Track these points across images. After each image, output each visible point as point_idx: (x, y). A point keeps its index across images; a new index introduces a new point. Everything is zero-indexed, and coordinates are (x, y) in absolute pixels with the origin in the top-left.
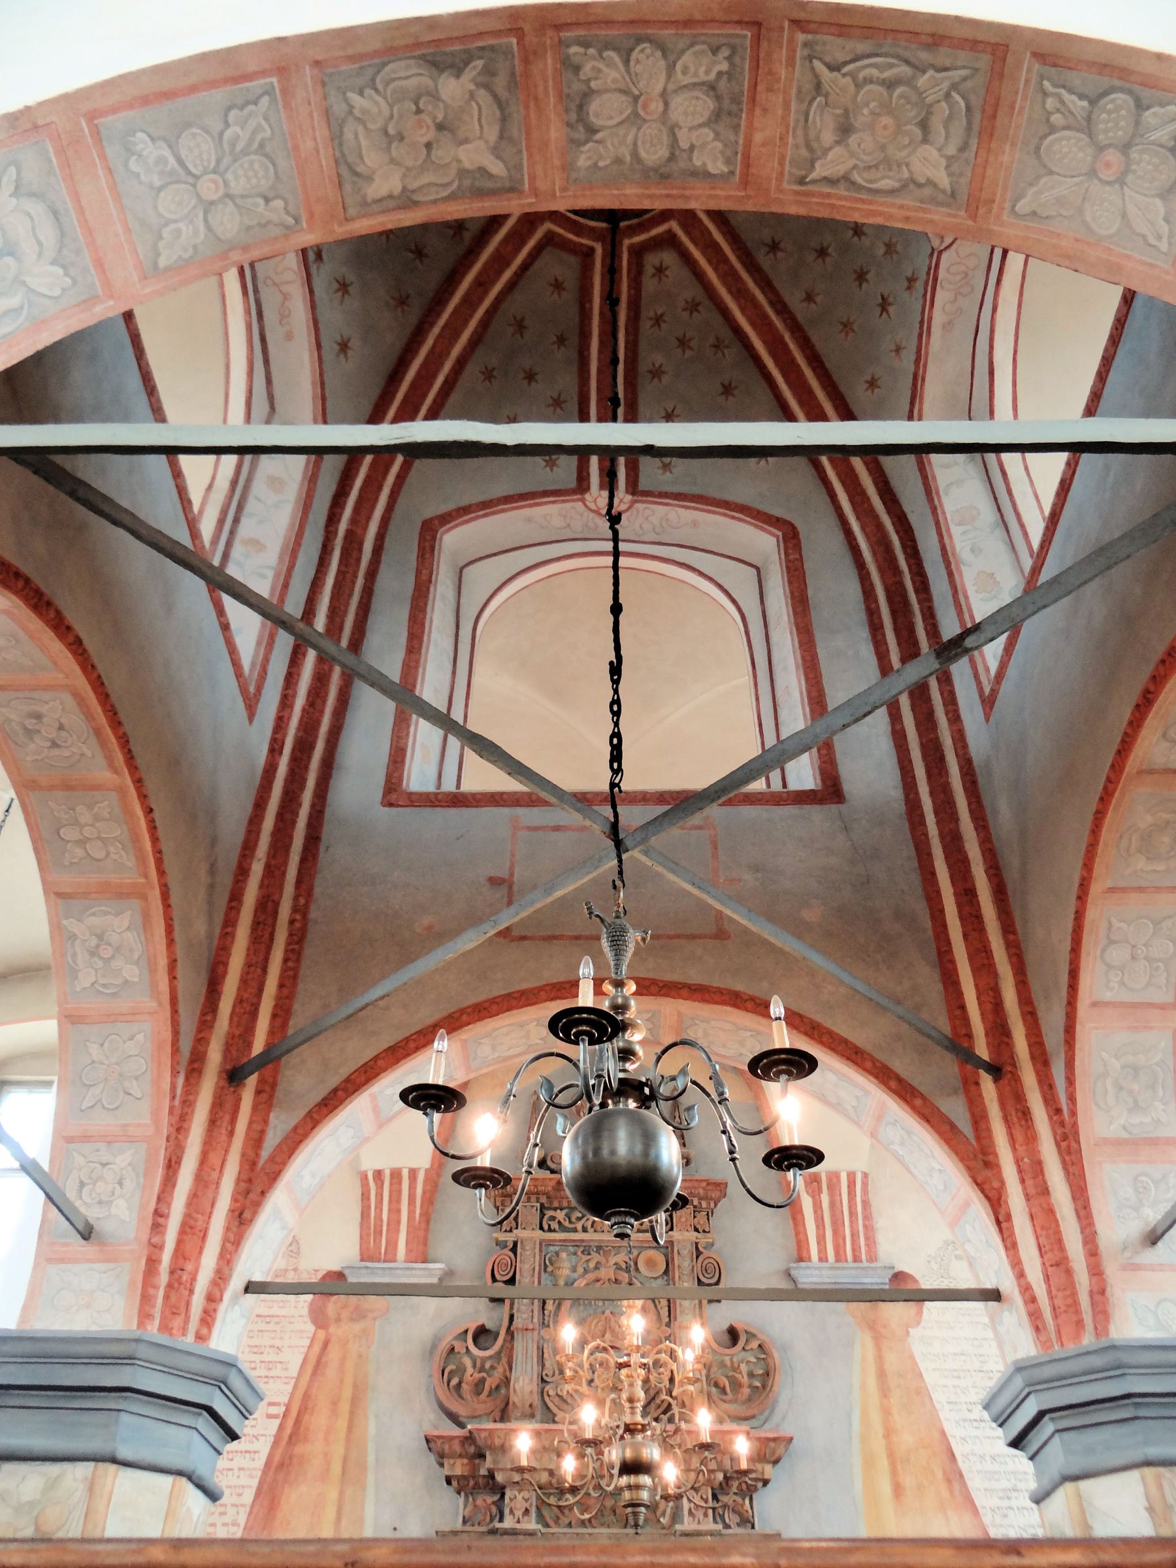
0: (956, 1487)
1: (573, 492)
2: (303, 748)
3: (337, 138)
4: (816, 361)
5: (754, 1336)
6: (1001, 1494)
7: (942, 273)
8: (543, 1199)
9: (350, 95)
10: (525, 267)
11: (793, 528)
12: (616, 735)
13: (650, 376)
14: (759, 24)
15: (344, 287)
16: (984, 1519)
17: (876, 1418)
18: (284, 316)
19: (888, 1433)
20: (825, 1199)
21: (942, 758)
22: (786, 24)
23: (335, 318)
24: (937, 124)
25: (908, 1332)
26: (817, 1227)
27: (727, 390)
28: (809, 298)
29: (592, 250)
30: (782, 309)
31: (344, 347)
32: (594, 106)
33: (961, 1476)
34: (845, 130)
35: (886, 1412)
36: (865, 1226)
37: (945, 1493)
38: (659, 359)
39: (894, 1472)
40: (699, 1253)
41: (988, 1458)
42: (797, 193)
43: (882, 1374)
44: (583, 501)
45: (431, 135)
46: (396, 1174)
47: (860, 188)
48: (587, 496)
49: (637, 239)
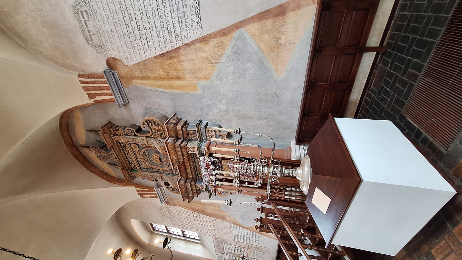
0: (172, 55)
5: (144, 123)
6: (170, 36)
8: (129, 171)
16: (181, 45)
17: (158, 83)
19: (162, 79)
20: (94, 92)
25: (126, 66)
26: (105, 95)
33: (168, 52)
35: (155, 79)
36: (97, 78)
37: (175, 60)
39: (172, 79)
40: (127, 135)
41: (159, 39)
43: (143, 78)
46: (139, 194)
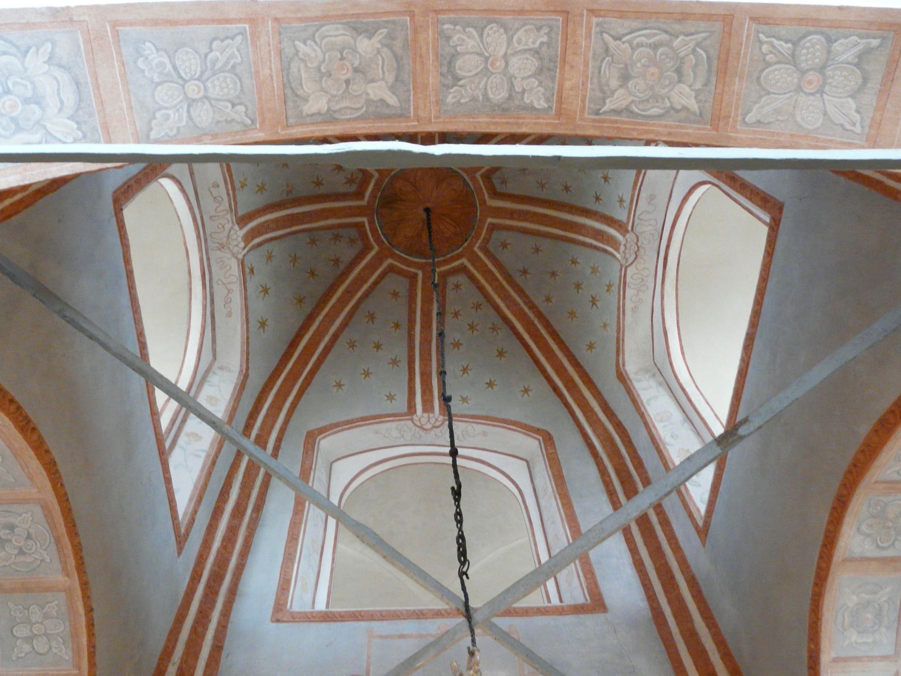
1: (405, 415)
2: (217, 578)
3: (285, 70)
4: (554, 334)
7: (628, 280)
9: (297, 43)
10: (376, 283)
11: (549, 434)
12: (461, 537)
13: (452, 347)
14: (568, 13)
15: (265, 291)
18: (228, 302)
21: (673, 578)
22: (585, 12)
23: (259, 307)
24: (688, 71)
27: (501, 354)
28: (548, 300)
29: (416, 274)
30: (532, 307)
31: (263, 324)
32: (459, 63)
34: (625, 78)
38: (458, 336)
42: (594, 121)
44: (412, 420)
45: (349, 75)
47: (637, 115)
48: (415, 417)
49: (443, 268)
